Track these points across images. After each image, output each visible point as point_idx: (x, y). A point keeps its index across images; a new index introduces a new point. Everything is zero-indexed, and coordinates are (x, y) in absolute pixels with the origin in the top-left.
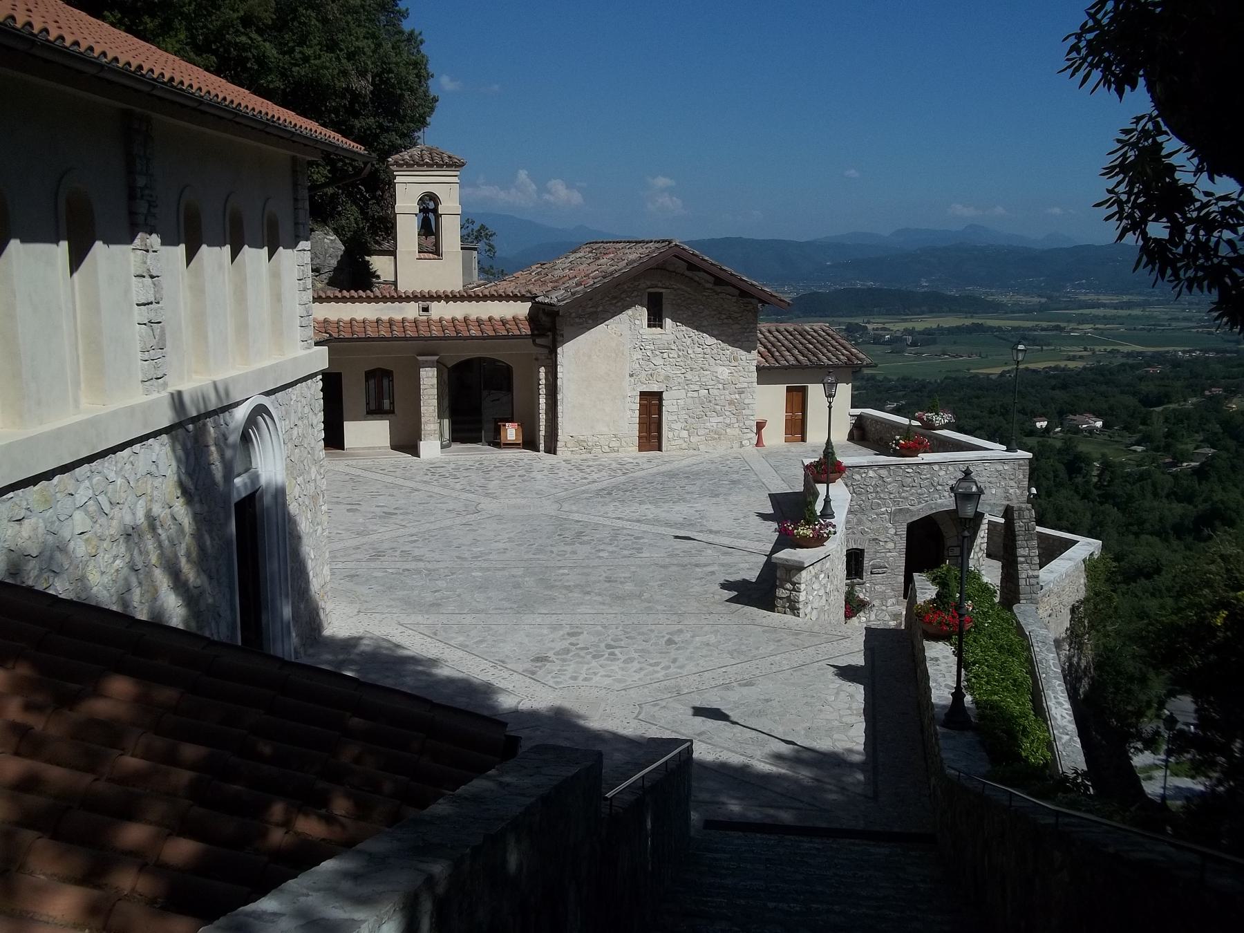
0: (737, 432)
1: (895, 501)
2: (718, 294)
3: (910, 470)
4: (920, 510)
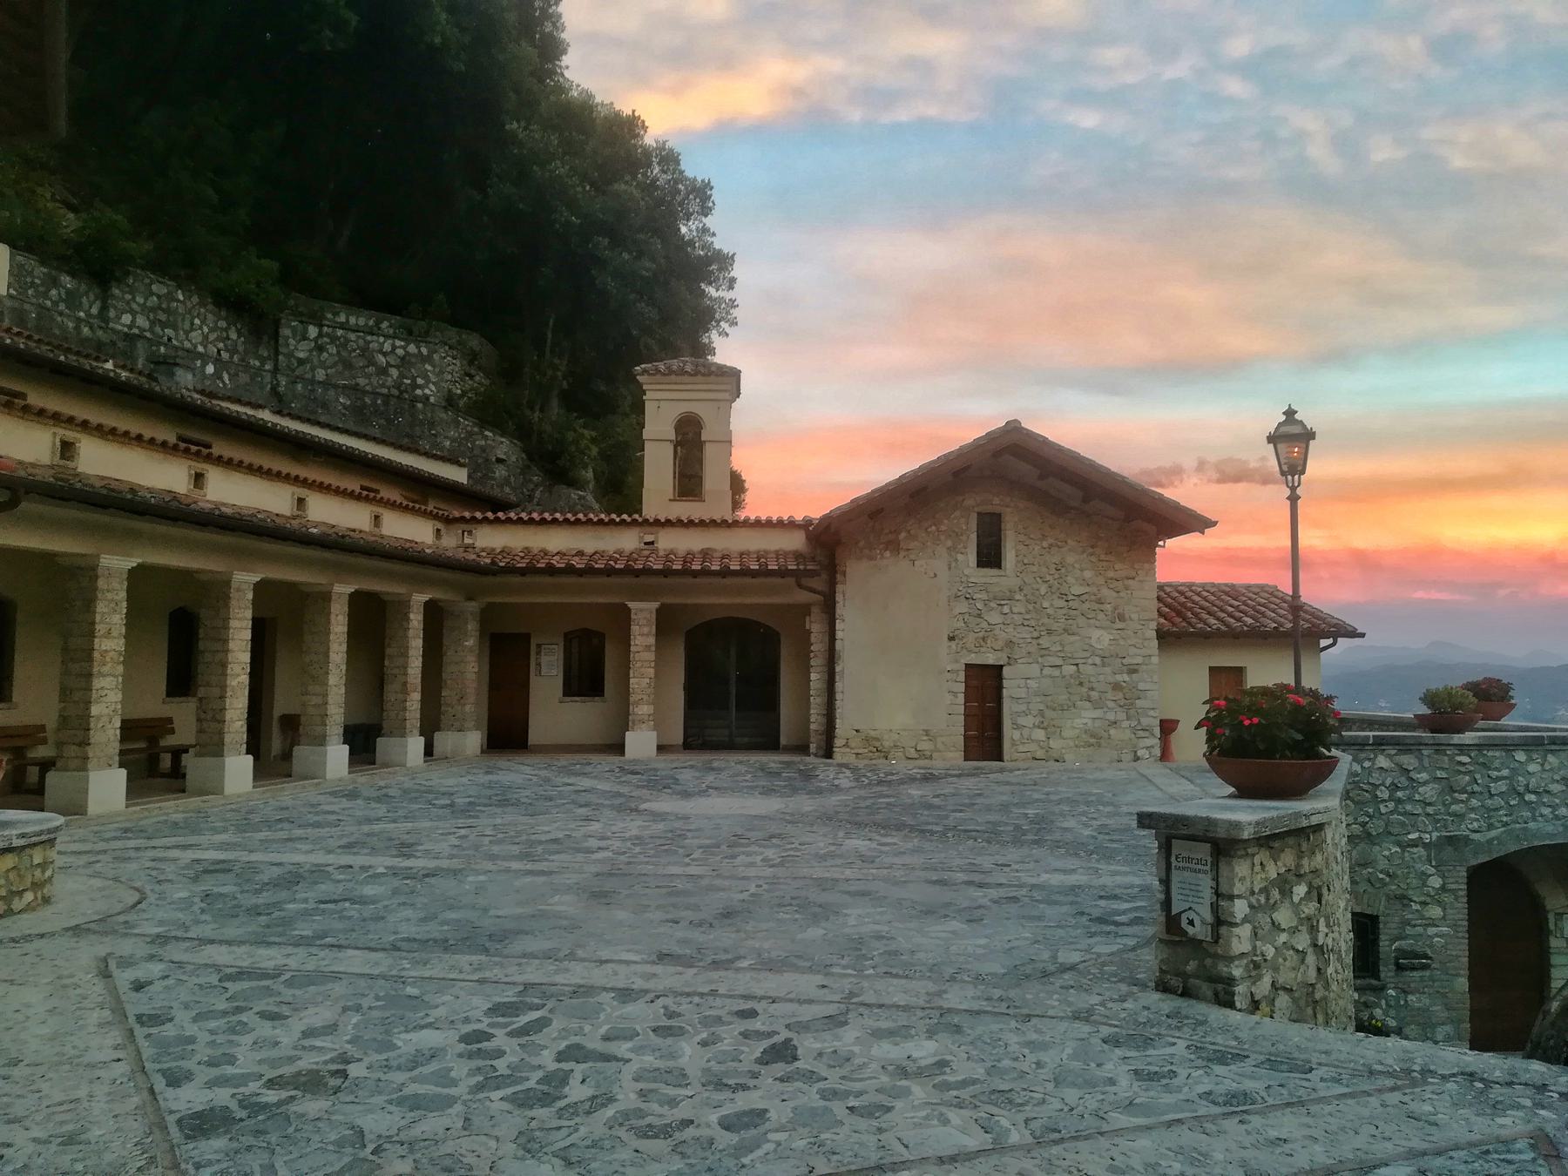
0: (1128, 734)
1: (1438, 821)
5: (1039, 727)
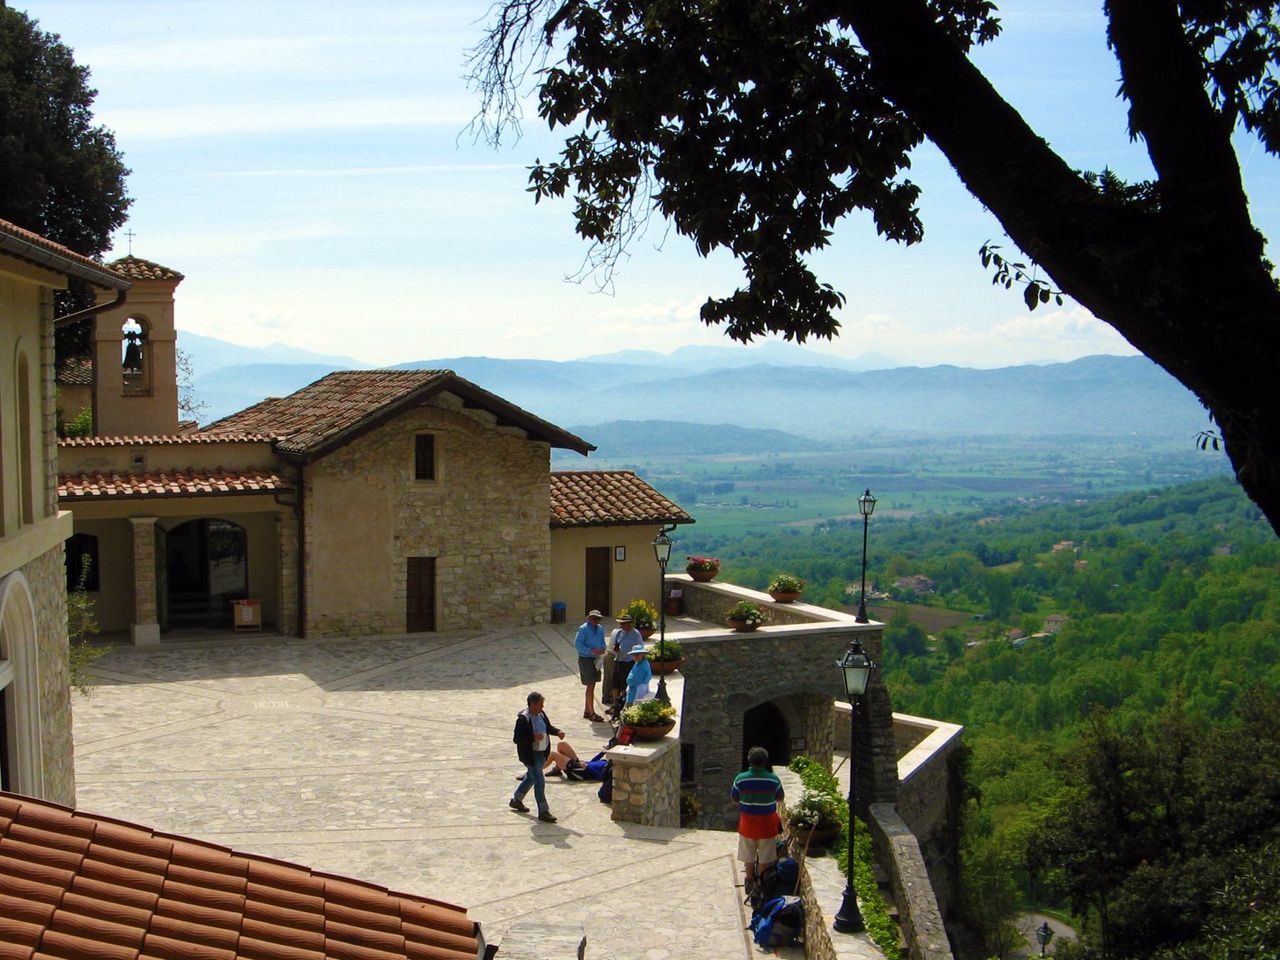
2: (501, 436)
3: (746, 648)
4: (759, 694)
5: (463, 604)
